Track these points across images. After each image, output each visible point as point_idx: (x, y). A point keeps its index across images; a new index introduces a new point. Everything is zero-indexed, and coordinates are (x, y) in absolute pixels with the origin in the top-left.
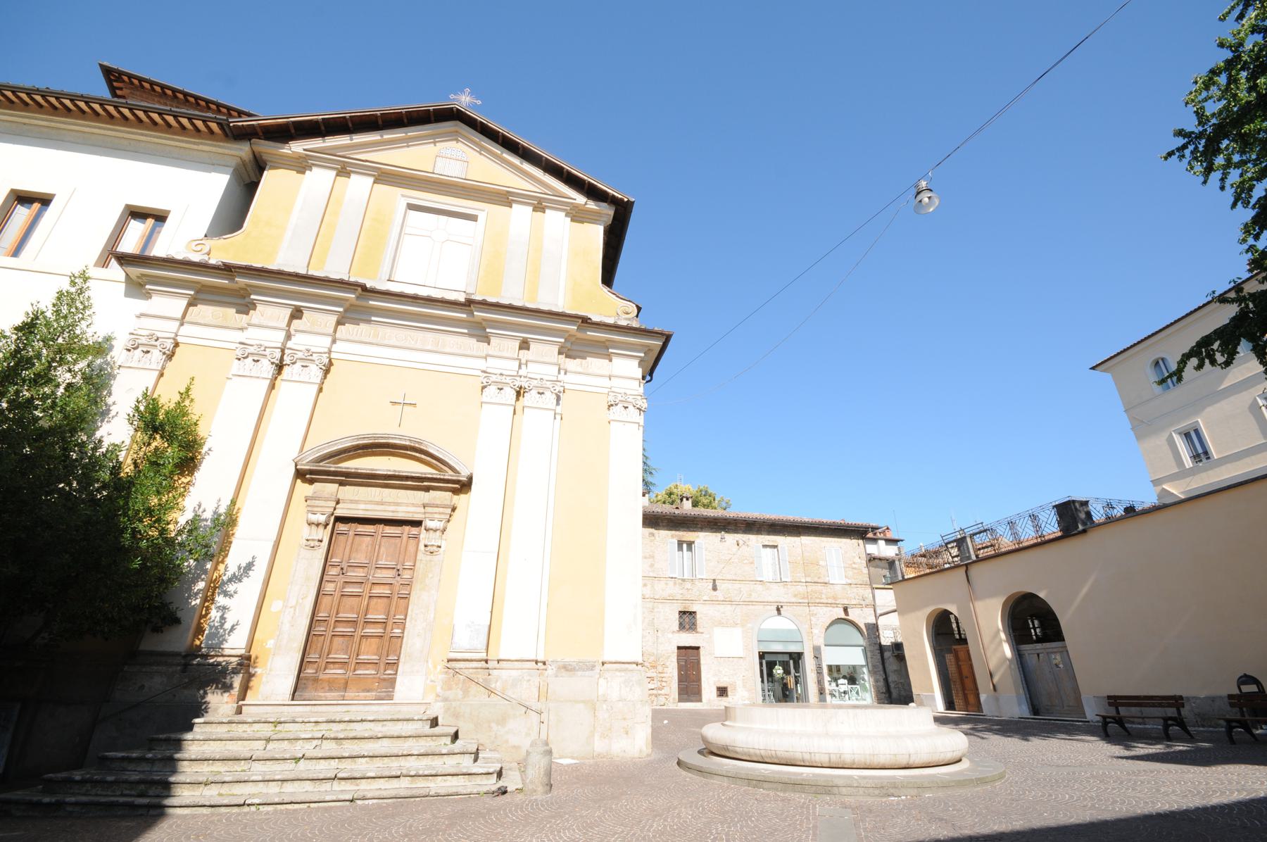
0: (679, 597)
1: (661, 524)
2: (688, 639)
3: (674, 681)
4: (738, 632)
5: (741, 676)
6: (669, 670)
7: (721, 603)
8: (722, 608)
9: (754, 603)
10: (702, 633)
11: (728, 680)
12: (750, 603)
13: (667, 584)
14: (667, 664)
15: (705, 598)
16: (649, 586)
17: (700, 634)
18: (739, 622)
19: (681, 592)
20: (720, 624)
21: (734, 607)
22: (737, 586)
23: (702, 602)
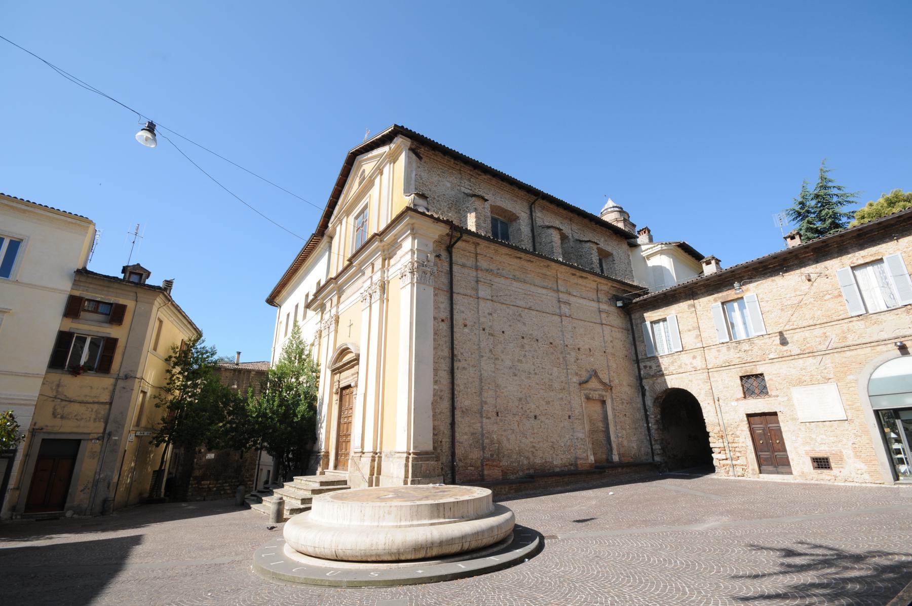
0: (736, 361)
1: (699, 292)
2: (758, 405)
3: (749, 451)
4: (831, 390)
5: (850, 444)
6: (741, 440)
7: (796, 357)
8: (800, 363)
9: (852, 348)
10: (777, 396)
11: (827, 449)
12: (846, 349)
13: (719, 351)
14: (738, 433)
15: (771, 356)
16: (699, 358)
17: (773, 398)
18: (831, 376)
19: (738, 355)
20: (800, 382)
21: (820, 358)
22: (818, 331)
23: (767, 361)
